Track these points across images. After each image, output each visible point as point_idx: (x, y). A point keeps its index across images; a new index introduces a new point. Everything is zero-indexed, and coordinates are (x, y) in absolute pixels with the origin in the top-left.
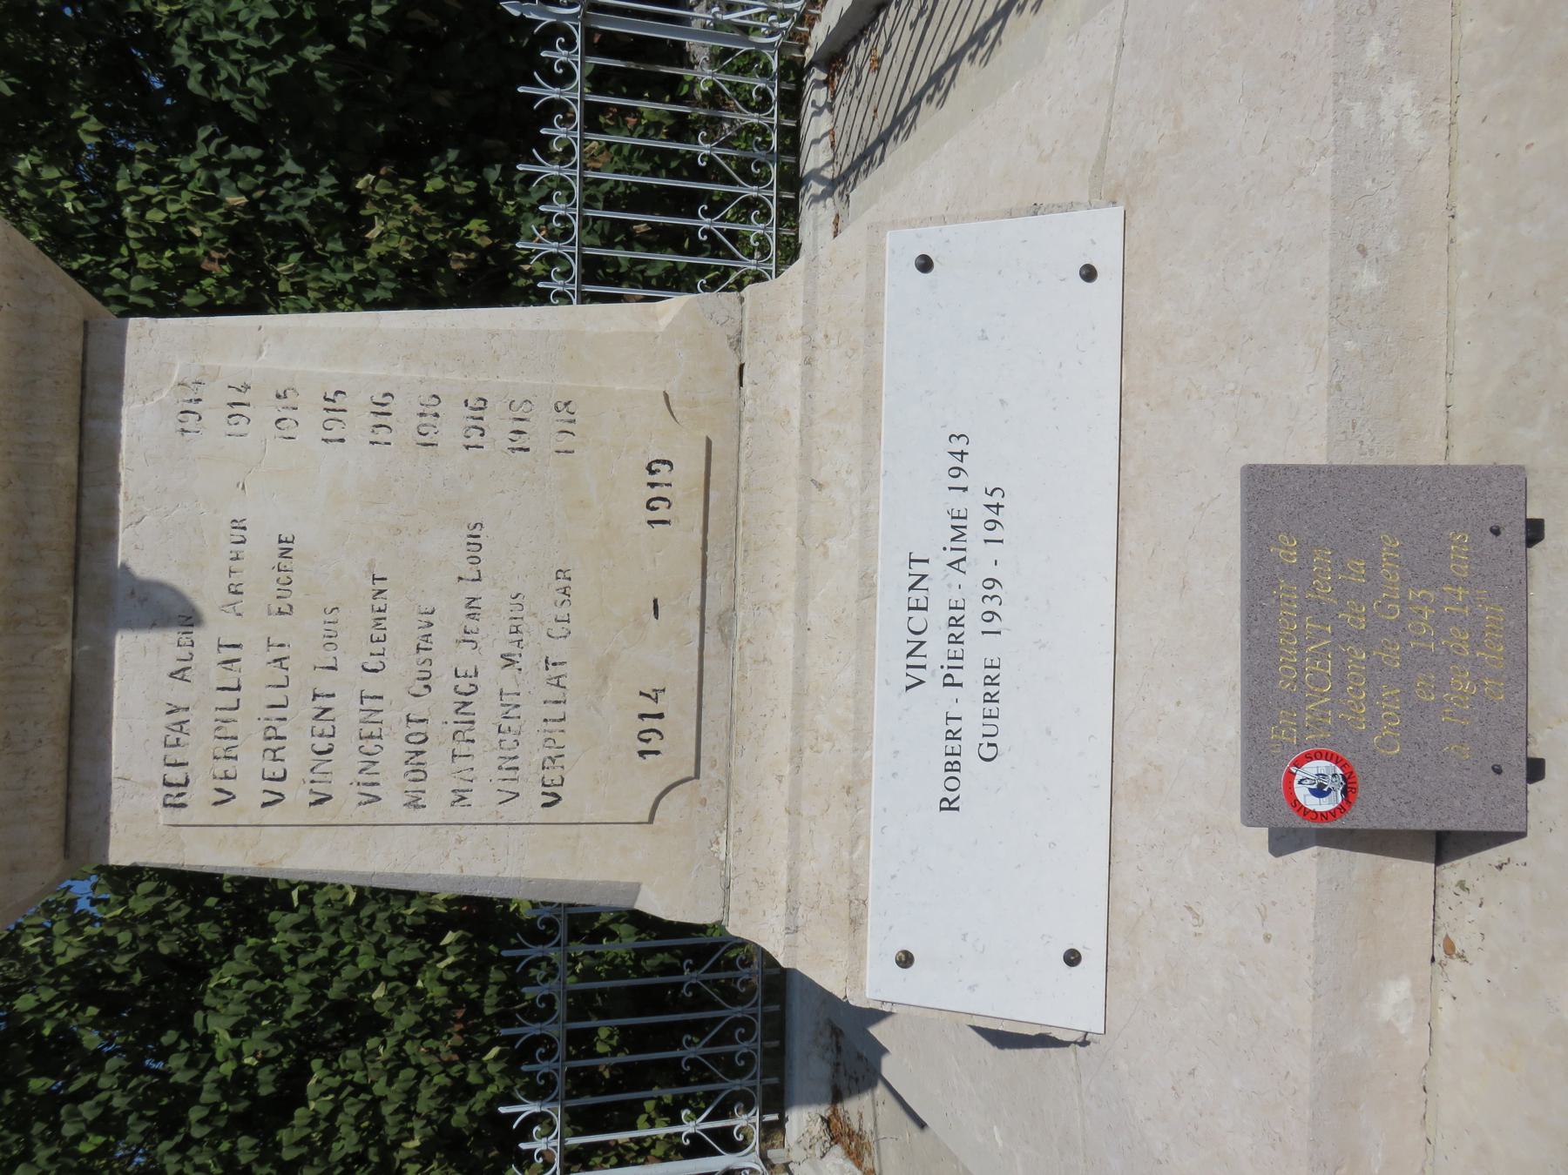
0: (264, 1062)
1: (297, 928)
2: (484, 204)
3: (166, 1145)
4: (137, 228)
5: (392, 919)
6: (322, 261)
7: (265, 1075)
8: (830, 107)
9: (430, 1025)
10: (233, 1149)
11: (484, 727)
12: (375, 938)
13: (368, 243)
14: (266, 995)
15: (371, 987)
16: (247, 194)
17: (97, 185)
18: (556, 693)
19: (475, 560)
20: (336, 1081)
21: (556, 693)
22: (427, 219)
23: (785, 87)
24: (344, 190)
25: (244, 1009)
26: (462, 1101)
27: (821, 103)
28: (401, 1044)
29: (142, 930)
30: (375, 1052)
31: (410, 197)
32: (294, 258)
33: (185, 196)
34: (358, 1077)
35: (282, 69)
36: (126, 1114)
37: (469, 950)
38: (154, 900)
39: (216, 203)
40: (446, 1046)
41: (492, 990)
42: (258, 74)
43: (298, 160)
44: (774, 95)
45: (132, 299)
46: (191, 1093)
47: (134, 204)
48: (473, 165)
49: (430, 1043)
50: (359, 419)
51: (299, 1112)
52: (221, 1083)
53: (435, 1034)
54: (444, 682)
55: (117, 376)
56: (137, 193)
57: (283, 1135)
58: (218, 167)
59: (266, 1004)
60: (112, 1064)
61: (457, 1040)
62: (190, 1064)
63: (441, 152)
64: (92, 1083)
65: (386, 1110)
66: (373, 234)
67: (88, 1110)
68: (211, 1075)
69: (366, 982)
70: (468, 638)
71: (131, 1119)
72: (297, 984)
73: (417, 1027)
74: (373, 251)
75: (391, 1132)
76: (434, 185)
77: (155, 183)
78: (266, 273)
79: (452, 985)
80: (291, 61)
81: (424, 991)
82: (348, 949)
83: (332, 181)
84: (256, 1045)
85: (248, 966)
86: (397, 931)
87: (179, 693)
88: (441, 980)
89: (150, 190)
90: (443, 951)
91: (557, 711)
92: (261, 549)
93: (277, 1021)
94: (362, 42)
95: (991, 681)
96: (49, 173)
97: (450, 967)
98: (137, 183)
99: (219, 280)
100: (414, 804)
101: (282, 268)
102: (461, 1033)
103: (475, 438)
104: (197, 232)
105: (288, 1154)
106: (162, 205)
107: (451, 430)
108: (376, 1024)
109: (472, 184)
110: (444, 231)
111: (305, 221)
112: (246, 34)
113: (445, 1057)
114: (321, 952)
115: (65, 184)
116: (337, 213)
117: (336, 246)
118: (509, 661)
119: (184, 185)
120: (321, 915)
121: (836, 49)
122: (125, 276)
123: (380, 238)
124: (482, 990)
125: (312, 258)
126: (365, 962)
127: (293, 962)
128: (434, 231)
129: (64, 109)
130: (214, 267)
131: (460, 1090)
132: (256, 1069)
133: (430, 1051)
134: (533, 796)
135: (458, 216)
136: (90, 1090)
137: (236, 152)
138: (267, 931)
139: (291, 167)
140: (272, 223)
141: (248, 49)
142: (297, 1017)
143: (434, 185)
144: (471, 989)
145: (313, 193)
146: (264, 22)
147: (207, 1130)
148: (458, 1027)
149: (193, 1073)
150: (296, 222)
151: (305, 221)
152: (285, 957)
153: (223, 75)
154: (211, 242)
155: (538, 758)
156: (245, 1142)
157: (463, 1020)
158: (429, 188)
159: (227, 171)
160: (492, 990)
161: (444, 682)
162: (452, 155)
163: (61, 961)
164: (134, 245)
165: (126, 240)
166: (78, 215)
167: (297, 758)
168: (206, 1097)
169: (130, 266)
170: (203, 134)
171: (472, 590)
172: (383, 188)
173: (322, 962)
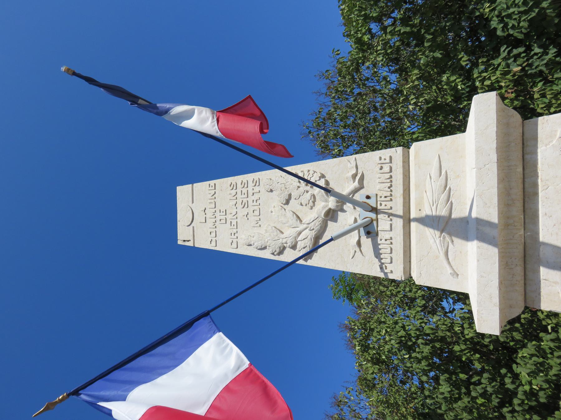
7: (541, 394)
14: (542, 364)
16: (520, 65)
25: (534, 367)
33: (498, 73)
35: (533, 14)
36: (491, 394)
39: (509, 72)
43: (539, 47)
46: (515, 394)
47: (480, 81)
52: (525, 392)
55: (535, 138)
56: (480, 76)
58: (509, 59)
60: (486, 375)
62: (513, 383)
64: (479, 380)
71: (494, 396)
77: (486, 72)
78: (529, 93)
80: (537, 10)
84: (538, 382)
85: (533, 351)
89: (485, 74)
93: (546, 375)
96: (453, 78)
101: (535, 89)
106: (489, 78)
127: (552, 353)
136: (479, 383)
137: (515, 51)
139: (537, 50)
140: (531, 74)
141: (519, 12)
142: (555, 375)
145: (547, 57)
147: (521, 409)
149: (514, 386)
152: (548, 351)
153: (510, 25)
159: (513, 59)
163: (467, 337)
168: (520, 396)
170: (502, 49)
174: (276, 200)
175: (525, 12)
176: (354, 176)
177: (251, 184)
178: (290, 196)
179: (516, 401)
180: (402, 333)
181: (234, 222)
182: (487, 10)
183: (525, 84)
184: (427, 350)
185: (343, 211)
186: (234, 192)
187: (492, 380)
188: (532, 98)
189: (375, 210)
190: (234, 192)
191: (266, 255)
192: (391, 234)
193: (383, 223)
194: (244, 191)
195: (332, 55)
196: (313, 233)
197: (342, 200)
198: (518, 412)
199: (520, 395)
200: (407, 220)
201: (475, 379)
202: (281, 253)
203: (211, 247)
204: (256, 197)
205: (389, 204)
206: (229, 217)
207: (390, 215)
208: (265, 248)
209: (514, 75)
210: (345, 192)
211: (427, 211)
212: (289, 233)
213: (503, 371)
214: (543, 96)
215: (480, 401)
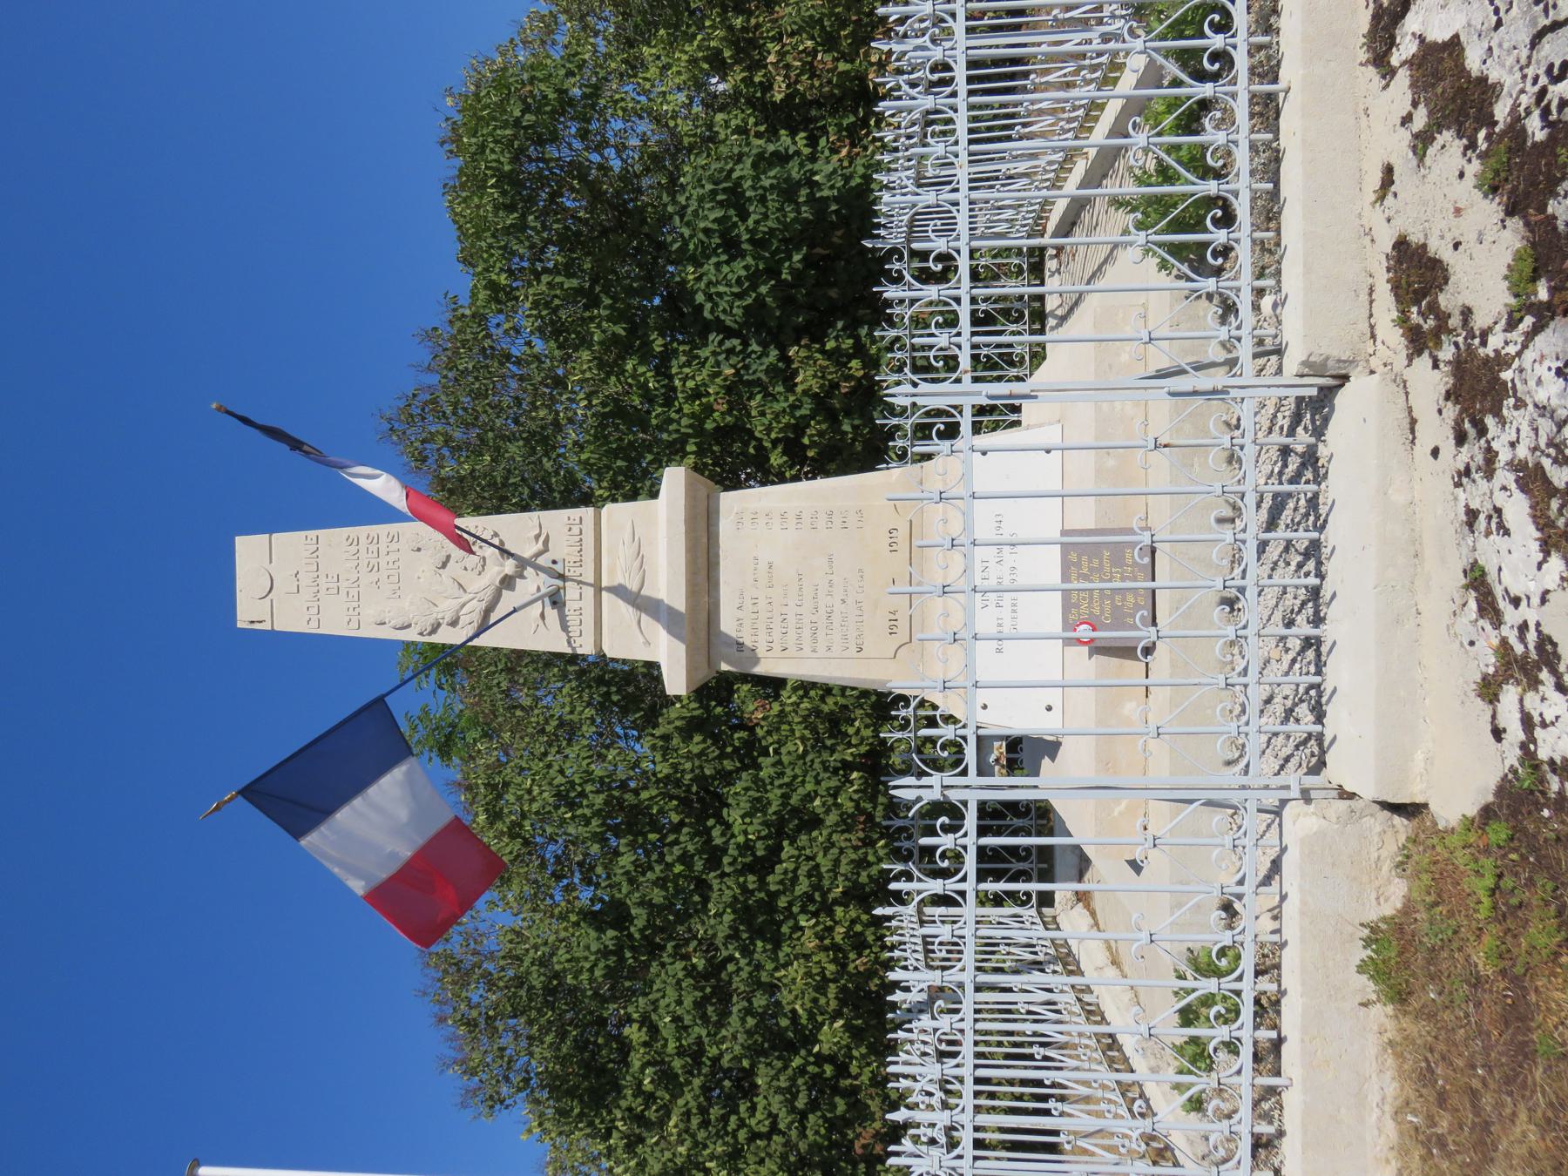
0: (759, 838)
1: (774, 765)
2: (859, 350)
3: (712, 874)
4: (682, 392)
5: (823, 763)
6: (775, 399)
7: (759, 845)
8: (1058, 271)
9: (846, 823)
10: (745, 881)
11: (836, 624)
12: (814, 773)
13: (796, 385)
14: (758, 800)
15: (812, 800)
17: (663, 371)
18: (860, 613)
19: (831, 567)
20: (796, 853)
21: (860, 613)
22: (827, 367)
23: (1032, 260)
24: (784, 357)
25: (749, 805)
26: (865, 869)
27: (1053, 269)
28: (830, 835)
29: (697, 763)
30: (815, 839)
31: (818, 355)
32: (759, 397)
33: (705, 372)
34: (808, 852)
35: (749, 301)
36: (693, 855)
37: (866, 782)
38: (702, 746)
39: (718, 374)
40: (855, 837)
41: (880, 808)
42: (738, 307)
43: (759, 344)
44: (1025, 267)
45: (683, 430)
46: (724, 850)
47: (680, 380)
48: (851, 329)
49: (846, 835)
50: (792, 521)
51: (777, 867)
52: (738, 846)
53: (848, 831)
54: (822, 610)
55: (717, 512)
56: (681, 373)
57: (770, 878)
58: (719, 354)
59: (758, 806)
60: (685, 830)
61: (861, 835)
63: (832, 325)
64: (677, 839)
65: (823, 870)
66: (798, 380)
67: (677, 851)
68: (732, 841)
69: (809, 798)
70: (830, 594)
71: (696, 858)
72: (774, 795)
73: (837, 824)
74: (799, 389)
75: (826, 883)
76: (830, 345)
78: (745, 407)
79: (857, 802)
80: (754, 295)
81: (842, 805)
82: (800, 779)
83: (777, 352)
84: (756, 826)
85: (749, 784)
86: (826, 769)
87: (740, 614)
88: (851, 799)
89: (687, 370)
90: (852, 783)
91: (860, 619)
92: (763, 566)
93: (765, 814)
94: (789, 278)
95: (1014, 605)
96: (641, 369)
97: (855, 791)
98: (680, 367)
99: (722, 413)
100: (814, 651)
101: (753, 403)
102: (863, 830)
103: (830, 525)
104: (711, 391)
105: (773, 888)
106: (693, 378)
107: (822, 523)
108: (815, 822)
109: (850, 341)
110: (836, 372)
111: (764, 378)
112: (731, 286)
113: (854, 843)
114: (786, 780)
115: (649, 374)
116: (780, 369)
117: (779, 389)
118: (843, 601)
119: (704, 363)
120: (785, 759)
121: (1070, 220)
122: (677, 417)
123: (802, 382)
124: (875, 808)
125: (769, 396)
126: (809, 787)
127: (772, 784)
128: (831, 373)
129: (646, 335)
130: (719, 407)
131: (862, 863)
132: (754, 842)
133: (846, 840)
134: (854, 649)
135: (845, 360)
136: (676, 842)
137: (728, 344)
138: (759, 768)
139: (755, 347)
140: (748, 381)
141: (733, 294)
142: (774, 813)
143: (830, 345)
144: (868, 806)
145: (766, 361)
146: (739, 279)
147: (732, 869)
148: (861, 826)
149: (724, 839)
150: (759, 379)
151: (764, 378)
152: (768, 781)
153: (721, 308)
154: (718, 393)
155: (855, 634)
156: (751, 878)
157: (864, 823)
158: (828, 347)
159: (724, 356)
160: (880, 808)
161: (822, 610)
162: (840, 324)
163: (659, 776)
164: (681, 401)
165: (677, 398)
166: (656, 389)
167: (776, 635)
168: (731, 852)
169: (679, 411)
171: (830, 577)
172: (803, 353)
173: (787, 785)
174: (428, 561)
175: (739, 296)
176: (537, 537)
177: (383, 538)
178: (448, 557)
179: (726, 860)
180: (560, 780)
181: (354, 592)
182: (691, 277)
183: (741, 397)
184: (599, 800)
185: (522, 577)
186: (353, 549)
187: (692, 836)
188: (749, 415)
189: (562, 577)
190: (353, 549)
191: (411, 635)
192: (580, 604)
193: (571, 592)
194: (373, 548)
195: (443, 301)
196: (483, 605)
197: (523, 563)
198: (728, 875)
199: (732, 851)
200: (598, 589)
201: (671, 838)
202: (434, 631)
203: (311, 629)
204: (392, 557)
205: (579, 570)
206: (344, 585)
207: (579, 582)
208: (409, 626)
209: (725, 380)
210: (527, 554)
211: (619, 579)
212: (446, 608)
213: (711, 822)
214: (763, 414)
215: (678, 868)
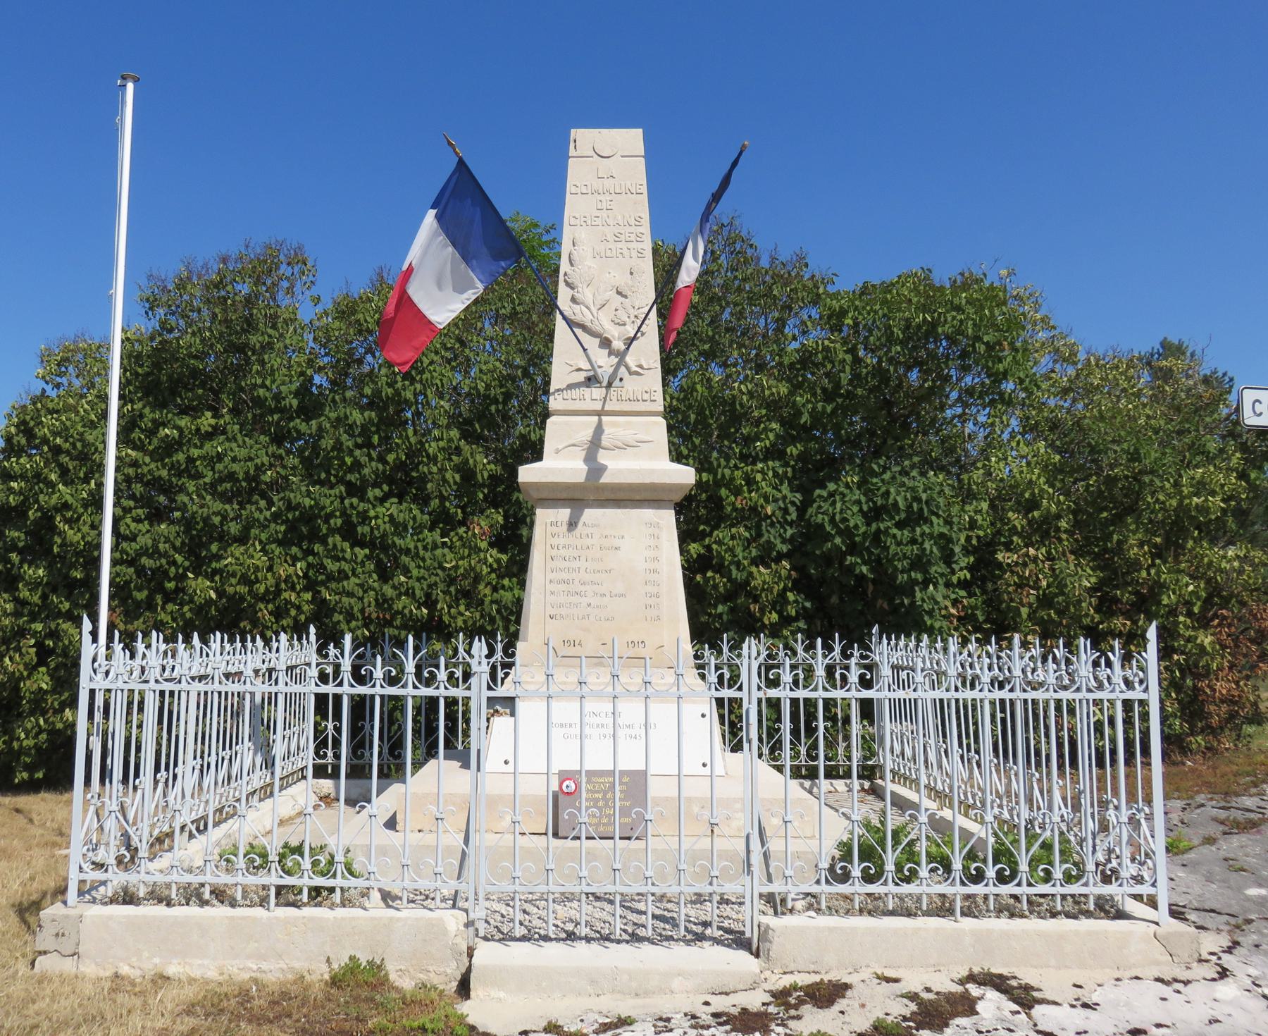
0: (372, 529)
2: (786, 621)
5: (436, 584)
7: (367, 529)
9: (383, 603)
13: (757, 566)
16: (773, 514)
17: (770, 453)
20: (359, 560)
26: (345, 618)
28: (374, 589)
30: (370, 576)
32: (747, 535)
33: (769, 490)
35: (828, 528)
40: (372, 610)
41: (396, 632)
43: (792, 536)
46: (362, 498)
48: (804, 614)
49: (373, 603)
50: (652, 566)
52: (366, 511)
53: (378, 604)
54: (582, 588)
55: (659, 508)
57: (338, 538)
60: (380, 467)
61: (374, 616)
62: (376, 498)
63: (807, 598)
65: (345, 583)
66: (761, 569)
69: (406, 572)
70: (595, 594)
72: (408, 542)
73: (383, 595)
74: (754, 569)
75: (333, 585)
76: (791, 596)
77: (774, 476)
78: (738, 523)
79: (401, 613)
83: (785, 550)
86: (430, 586)
88: (404, 607)
89: (771, 474)
90: (418, 608)
92: (617, 543)
93: (393, 534)
96: (771, 436)
98: (773, 469)
99: (734, 504)
101: (742, 529)
102: (378, 617)
105: (330, 540)
106: (764, 479)
107: (650, 588)
108: (384, 576)
109: (793, 613)
111: (763, 539)
113: (367, 610)
114: (421, 553)
115: (767, 442)
117: (754, 553)
118: (589, 605)
120: (439, 552)
124: (397, 628)
125: (748, 543)
126: (415, 572)
127: (419, 540)
134: (550, 611)
136: (371, 459)
137: (792, 509)
139: (790, 532)
141: (834, 514)
142: (394, 542)
143: (791, 596)
144: (398, 622)
145: (778, 541)
151: (763, 539)
156: (339, 522)
158: (789, 594)
160: (396, 632)
161: (582, 588)
162: (808, 605)
167: (563, 552)
170: (798, 495)
172: (784, 573)
173: (417, 554)
174: (622, 280)
175: (832, 520)
176: (641, 366)
177: (640, 246)
178: (625, 297)
179: (355, 501)
180: (426, 362)
181: (598, 221)
182: (849, 479)
183: (748, 519)
184: (409, 395)
185: (610, 354)
186: (633, 222)
187: (376, 472)
188: (732, 526)
189: (609, 385)
190: (633, 222)
191: (564, 266)
192: (588, 400)
193: (597, 392)
194: (633, 237)
195: (830, 273)
196: (588, 324)
197: (621, 355)
198: (342, 502)
199: (362, 506)
200: (599, 414)
201: (374, 455)
202: (568, 284)
203: (570, 188)
204: (626, 252)
205: (614, 399)
206: (604, 214)
207: (605, 399)
208: (572, 265)
209: (762, 507)
210: (628, 359)
211: (608, 430)
212: (586, 294)
213: (386, 488)
214: (733, 538)
215: (348, 460)
